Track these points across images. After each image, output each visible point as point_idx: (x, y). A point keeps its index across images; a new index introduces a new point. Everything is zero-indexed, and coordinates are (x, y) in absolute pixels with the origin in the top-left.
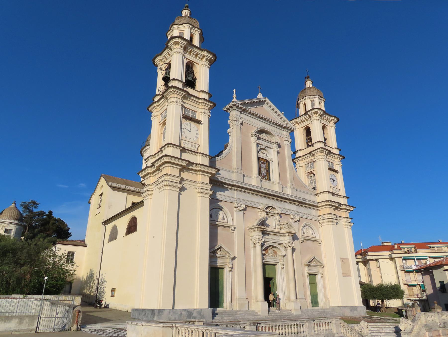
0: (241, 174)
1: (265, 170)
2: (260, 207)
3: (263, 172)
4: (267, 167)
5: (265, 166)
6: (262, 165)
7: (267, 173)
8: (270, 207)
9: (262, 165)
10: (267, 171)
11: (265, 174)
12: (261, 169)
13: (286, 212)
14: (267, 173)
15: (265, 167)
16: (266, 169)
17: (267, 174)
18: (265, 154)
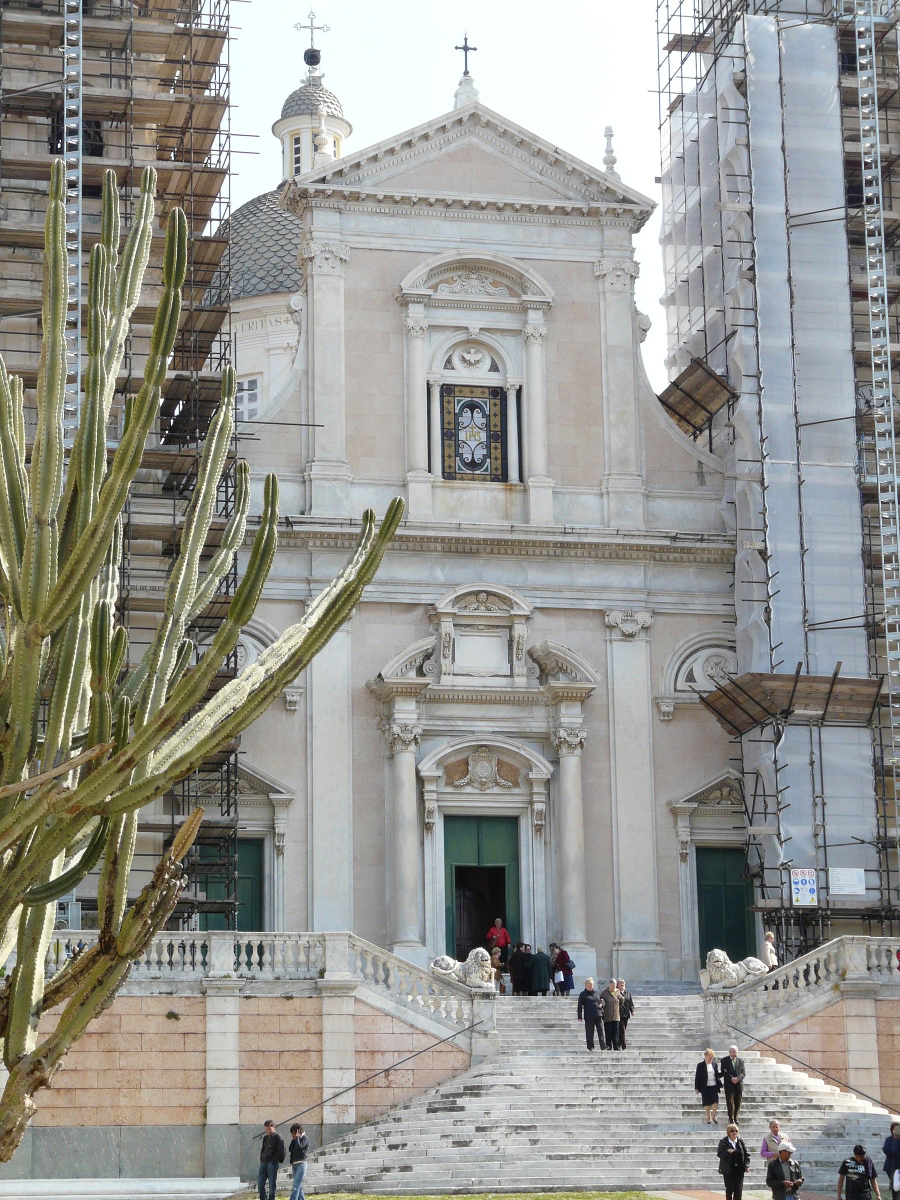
0: (334, 480)
1: (483, 436)
2: (426, 599)
3: (473, 444)
4: (497, 420)
5: (484, 415)
6: (467, 414)
7: (493, 445)
8: (477, 593)
9: (467, 414)
10: (492, 437)
11: (480, 453)
12: (462, 436)
13: (582, 602)
14: (493, 445)
15: (484, 420)
16: (488, 425)
17: (496, 448)
18: (487, 364)
